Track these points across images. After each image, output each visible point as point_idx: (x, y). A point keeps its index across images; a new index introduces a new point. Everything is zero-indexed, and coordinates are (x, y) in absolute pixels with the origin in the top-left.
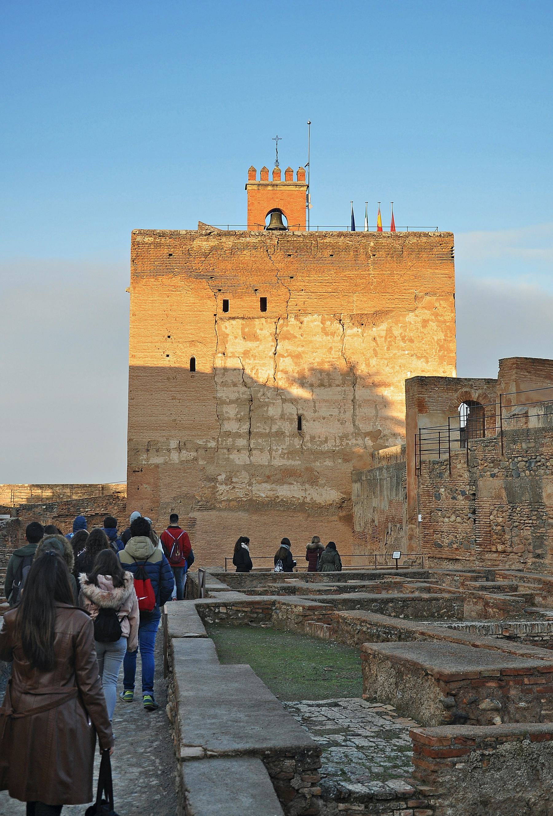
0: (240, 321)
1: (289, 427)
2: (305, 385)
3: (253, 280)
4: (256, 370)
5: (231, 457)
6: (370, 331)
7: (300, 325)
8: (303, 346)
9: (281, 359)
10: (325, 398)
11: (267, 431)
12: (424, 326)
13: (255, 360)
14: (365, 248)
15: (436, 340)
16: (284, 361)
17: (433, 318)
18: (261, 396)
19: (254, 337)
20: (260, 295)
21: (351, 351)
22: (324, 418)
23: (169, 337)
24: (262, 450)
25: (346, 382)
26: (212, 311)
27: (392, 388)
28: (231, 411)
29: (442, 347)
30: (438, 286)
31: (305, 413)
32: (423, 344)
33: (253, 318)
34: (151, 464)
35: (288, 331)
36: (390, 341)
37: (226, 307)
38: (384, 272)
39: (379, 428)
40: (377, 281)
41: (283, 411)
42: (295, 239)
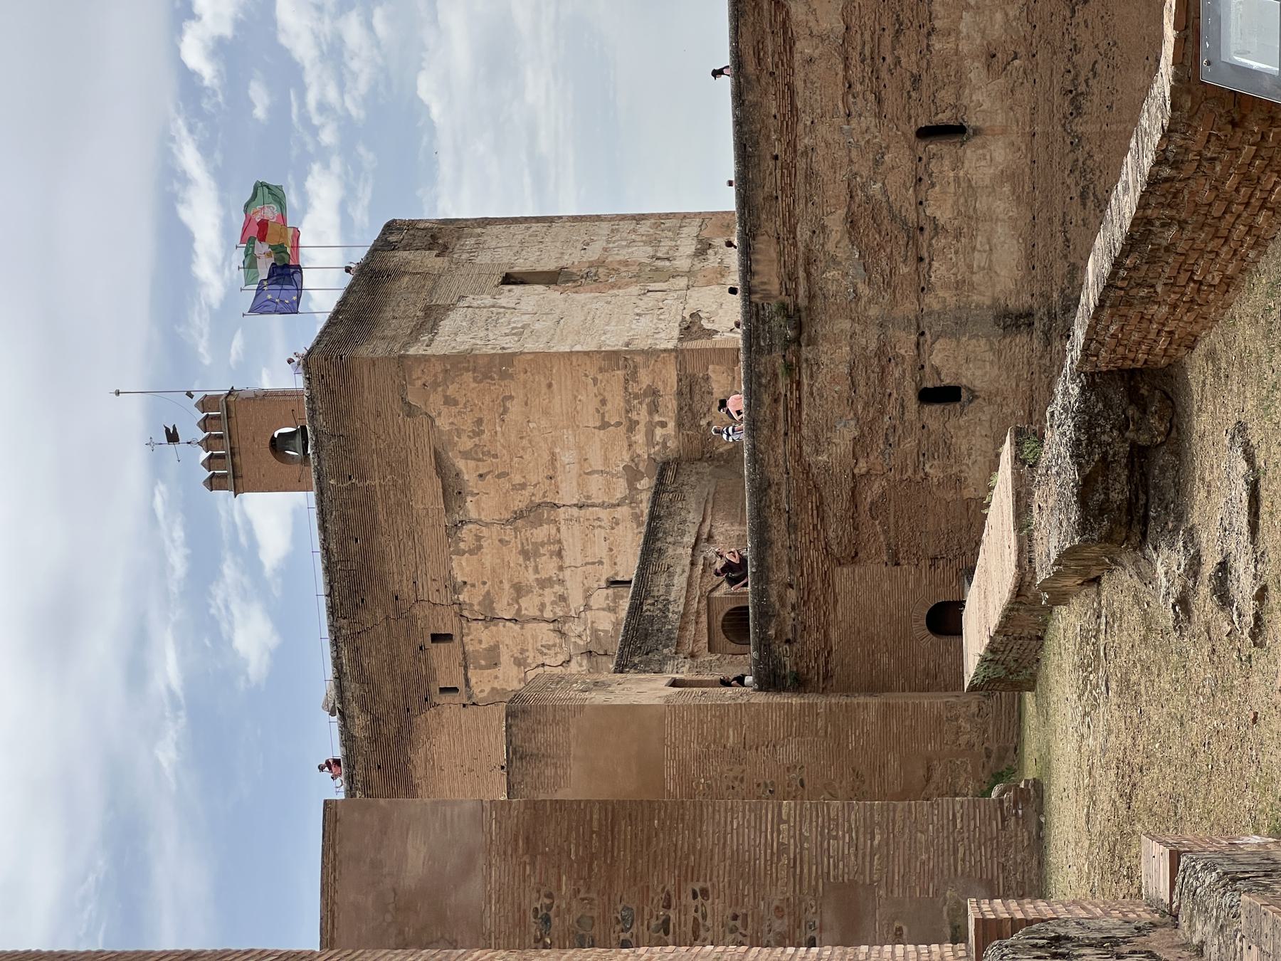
2: (561, 577)
4: (543, 649)
6: (471, 484)
7: (469, 586)
8: (501, 582)
9: (523, 612)
10: (579, 546)
12: (456, 403)
13: (527, 650)
14: (341, 491)
15: (477, 385)
16: (526, 609)
17: (440, 389)
18: (582, 639)
19: (493, 651)
21: (503, 511)
22: (611, 550)
25: (552, 518)
26: (459, 710)
27: (557, 450)
29: (487, 376)
30: (389, 382)
32: (483, 404)
35: (479, 604)
36: (482, 453)
38: (375, 462)
39: (621, 469)
40: (390, 474)
41: (603, 609)
42: (336, 594)
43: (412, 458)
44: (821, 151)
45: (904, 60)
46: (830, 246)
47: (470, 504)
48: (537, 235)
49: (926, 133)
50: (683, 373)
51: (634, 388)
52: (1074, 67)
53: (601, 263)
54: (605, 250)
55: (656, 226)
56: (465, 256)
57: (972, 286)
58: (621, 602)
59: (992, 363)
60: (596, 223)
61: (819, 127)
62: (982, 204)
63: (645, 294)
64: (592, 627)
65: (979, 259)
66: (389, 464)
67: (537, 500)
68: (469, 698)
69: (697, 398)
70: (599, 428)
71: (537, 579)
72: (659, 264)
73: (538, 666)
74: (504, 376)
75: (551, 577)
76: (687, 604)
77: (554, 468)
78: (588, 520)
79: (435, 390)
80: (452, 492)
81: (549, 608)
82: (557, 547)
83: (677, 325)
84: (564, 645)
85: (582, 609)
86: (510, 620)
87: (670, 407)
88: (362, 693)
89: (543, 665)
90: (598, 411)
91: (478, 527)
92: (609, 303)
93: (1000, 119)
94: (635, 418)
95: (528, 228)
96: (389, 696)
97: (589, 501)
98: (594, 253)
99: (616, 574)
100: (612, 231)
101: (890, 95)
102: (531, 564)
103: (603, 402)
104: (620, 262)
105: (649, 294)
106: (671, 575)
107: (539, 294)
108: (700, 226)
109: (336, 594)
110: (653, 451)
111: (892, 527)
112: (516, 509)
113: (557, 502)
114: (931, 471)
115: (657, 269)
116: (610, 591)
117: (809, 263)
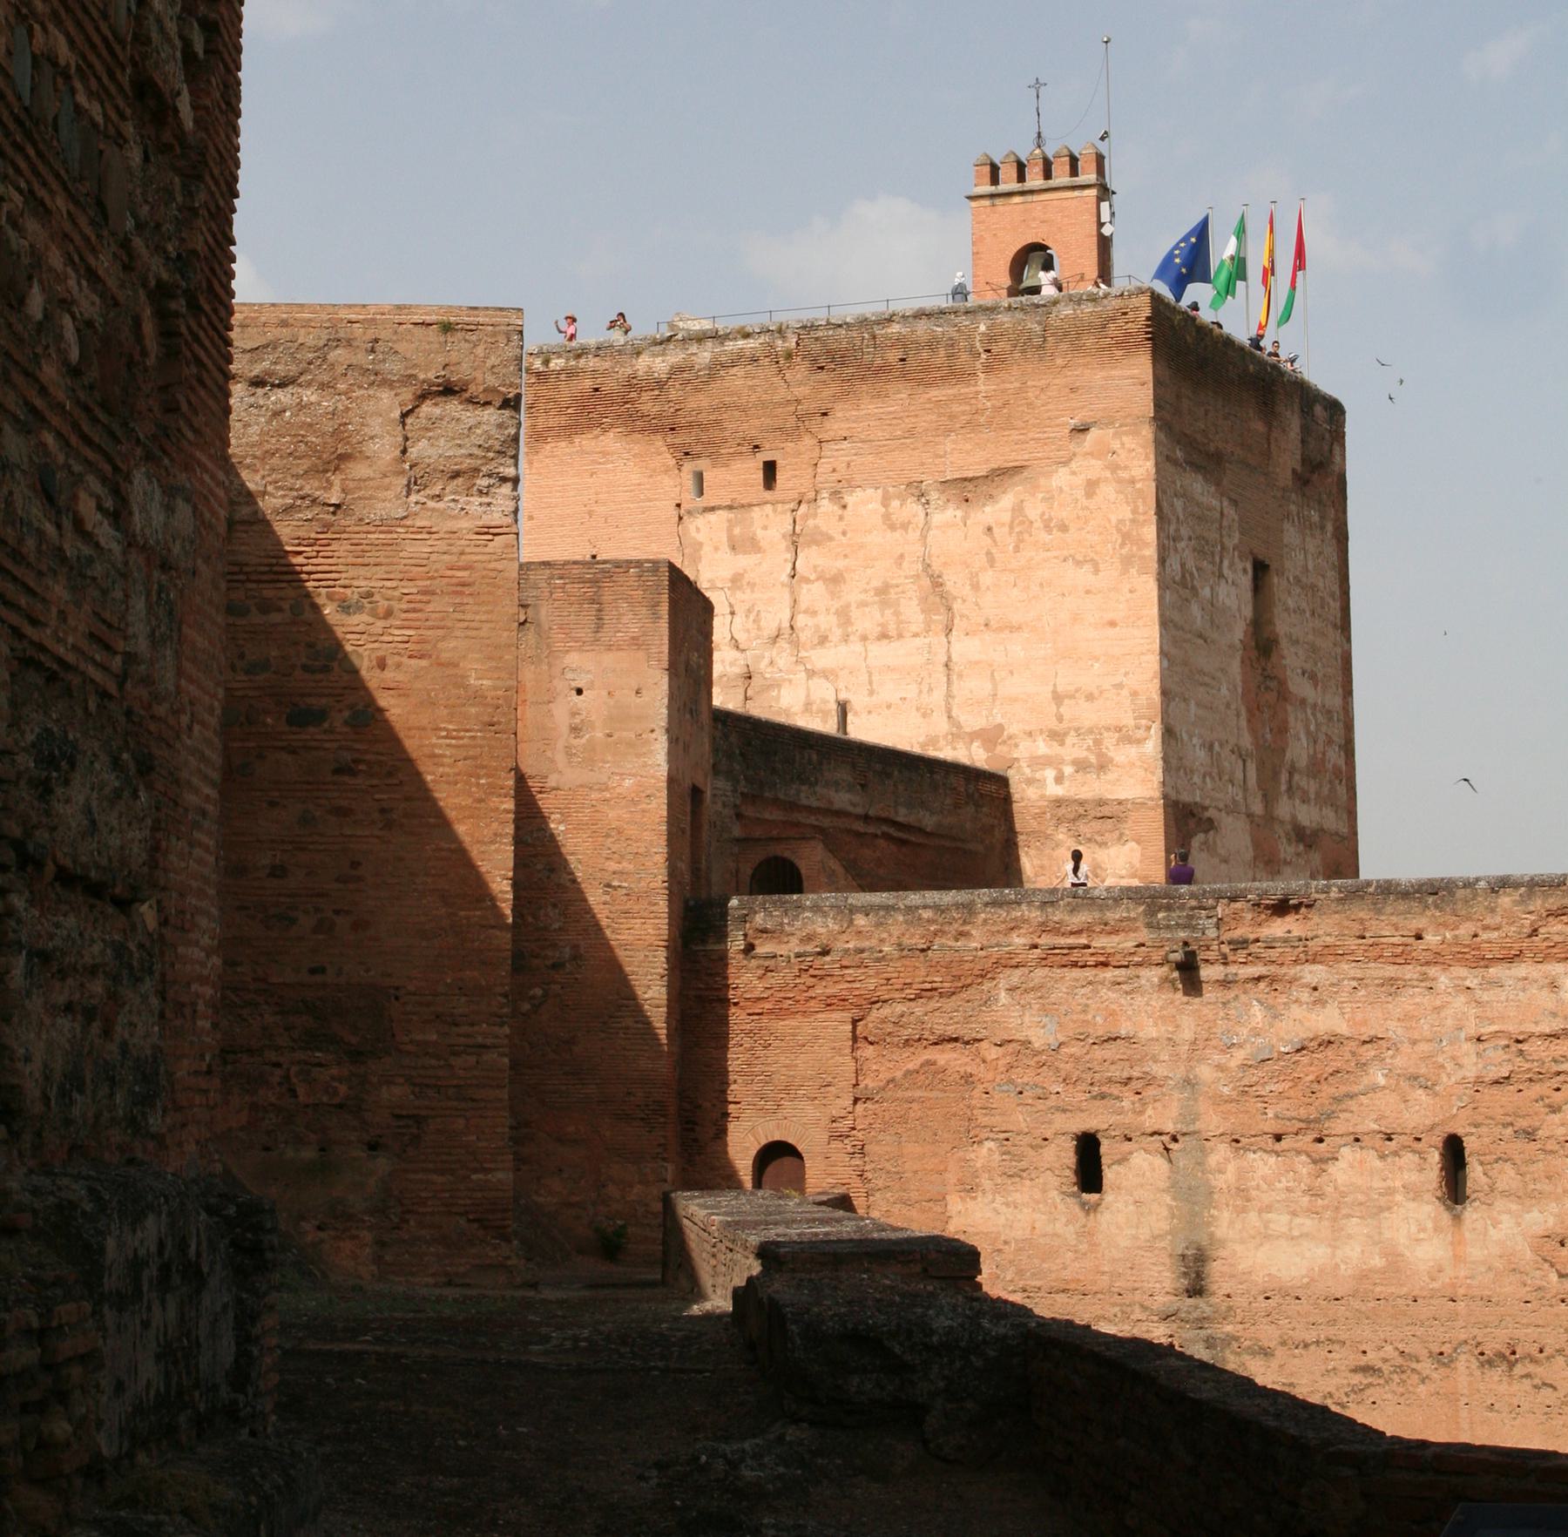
0: (723, 515)
2: (851, 638)
3: (752, 427)
7: (840, 512)
9: (805, 586)
14: (970, 338)
15: (1114, 521)
16: (809, 590)
22: (889, 707)
25: (933, 627)
29: (1126, 537)
33: (750, 505)
35: (816, 527)
38: (1008, 386)
40: (993, 406)
41: (808, 696)
43: (1015, 435)
44: (1426, 1000)
45: (1556, 1118)
46: (1296, 1011)
47: (952, 513)
48: (1323, 607)
49: (1454, 1152)
50: (1129, 806)
51: (1109, 740)
52: (1548, 1358)
53: (1283, 695)
54: (1303, 702)
55: (1337, 772)
56: (1293, 508)
57: (1244, 1210)
58: (818, 720)
59: (1135, 1238)
60: (1340, 690)
61: (1462, 999)
62: (1353, 1225)
63: (1241, 756)
64: (784, 680)
65: (1280, 1221)
67: (957, 606)
68: (689, 512)
69: (1097, 825)
70: (1054, 692)
71: (848, 606)
72: (1284, 777)
74: (1127, 562)
75: (852, 624)
76: (810, 810)
77: (1000, 629)
78: (930, 675)
79: (1107, 467)
80: (967, 489)
81: (810, 621)
82: (893, 633)
83: (1198, 799)
84: (759, 641)
85: (809, 667)
86: (794, 568)
87: (1084, 789)
88: (697, 367)
89: (733, 613)
90: (1077, 690)
91: (921, 526)
92: (1228, 706)
93: (1475, 1253)
94: (1069, 740)
95: (1332, 595)
96: (692, 403)
97: (955, 677)
98: (1300, 687)
100: (1329, 712)
101: (1505, 1095)
102: (870, 597)
103: (1090, 697)
104: (1286, 722)
105: (1240, 763)
106: (850, 789)
107: (1239, 610)
108: (1337, 834)
109: (831, 332)
110: (1024, 765)
111: (909, 1094)
112: (945, 577)
113: (954, 632)
114: (985, 1151)
115: (1276, 775)
116: (834, 706)
117: (1273, 980)
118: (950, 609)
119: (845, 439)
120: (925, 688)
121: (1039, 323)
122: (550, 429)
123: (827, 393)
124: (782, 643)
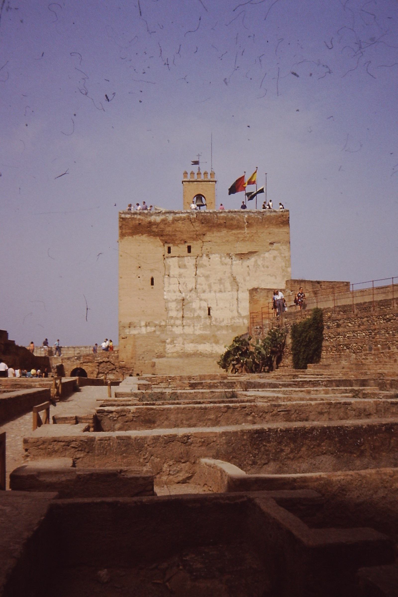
1: (204, 314)
2: (212, 291)
3: (184, 237)
5: (173, 330)
7: (209, 259)
9: (199, 278)
11: (192, 316)
19: (185, 266)
20: (187, 245)
22: (222, 309)
23: (140, 267)
24: (189, 326)
28: (173, 305)
29: (283, 270)
31: (211, 306)
33: (184, 257)
34: (131, 335)
37: (169, 252)
41: (200, 305)
43: (255, 244)
66: (252, 236)
67: (240, 285)
73: (179, 282)
80: (242, 256)
82: (223, 291)
86: (196, 273)
89: (179, 284)
99: (213, 310)
109: (205, 214)
113: (239, 291)
118: (238, 285)
119: (210, 241)
120: (231, 305)
121: (261, 216)
122: (126, 233)
123: (205, 229)
124: (193, 292)
